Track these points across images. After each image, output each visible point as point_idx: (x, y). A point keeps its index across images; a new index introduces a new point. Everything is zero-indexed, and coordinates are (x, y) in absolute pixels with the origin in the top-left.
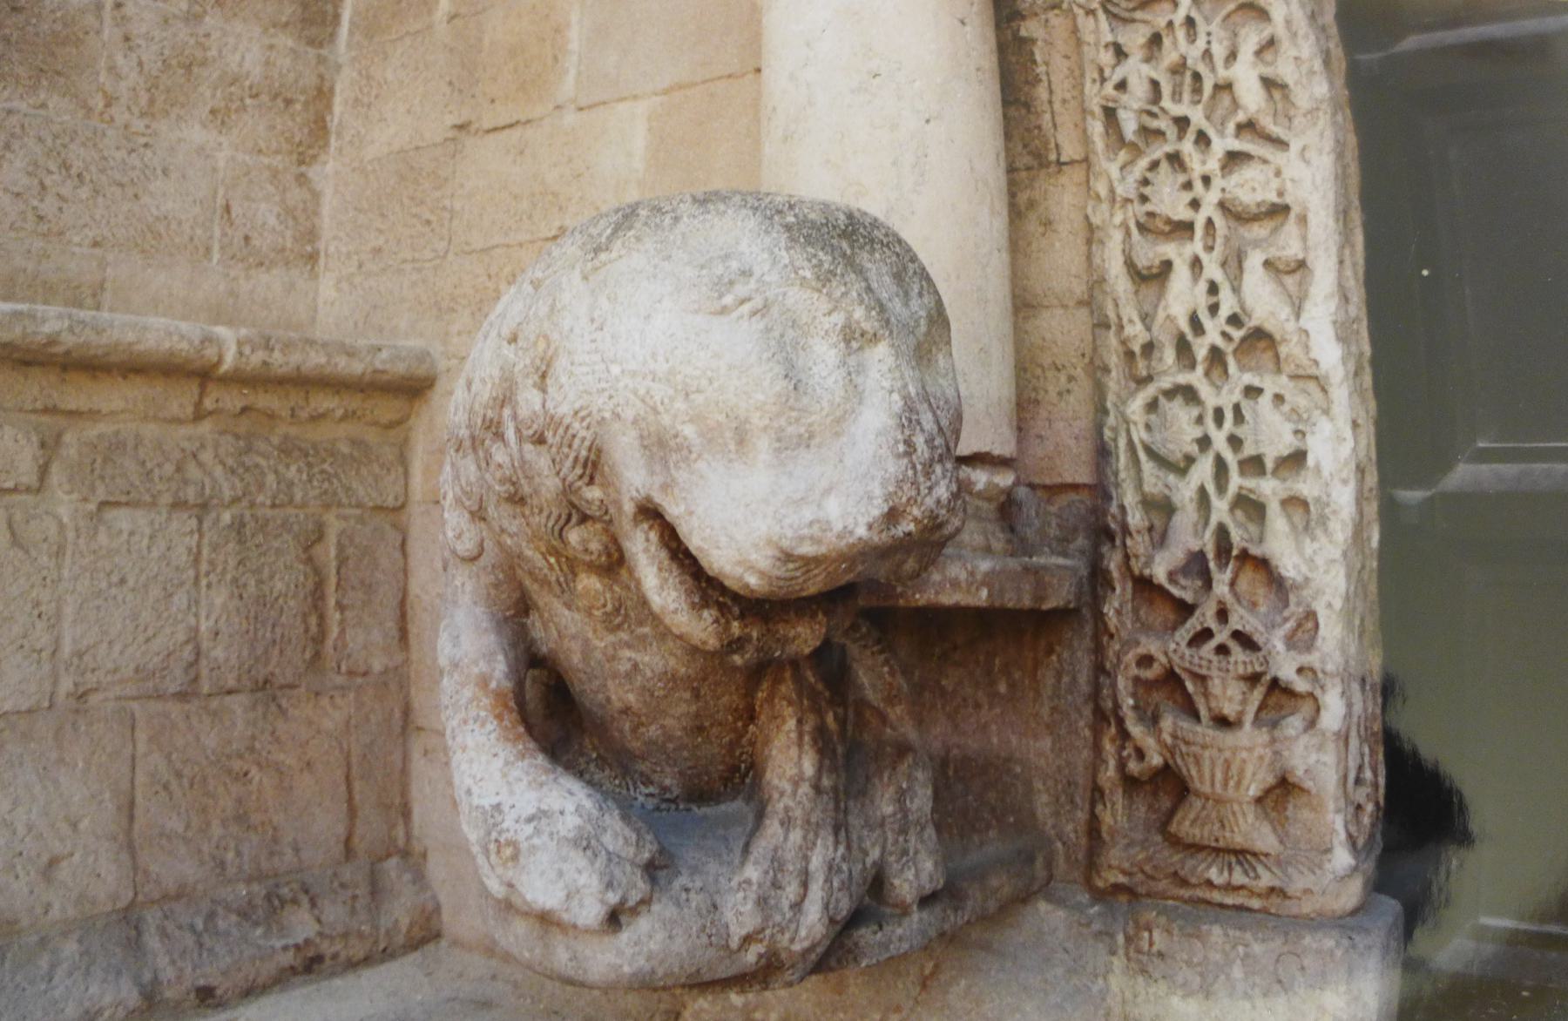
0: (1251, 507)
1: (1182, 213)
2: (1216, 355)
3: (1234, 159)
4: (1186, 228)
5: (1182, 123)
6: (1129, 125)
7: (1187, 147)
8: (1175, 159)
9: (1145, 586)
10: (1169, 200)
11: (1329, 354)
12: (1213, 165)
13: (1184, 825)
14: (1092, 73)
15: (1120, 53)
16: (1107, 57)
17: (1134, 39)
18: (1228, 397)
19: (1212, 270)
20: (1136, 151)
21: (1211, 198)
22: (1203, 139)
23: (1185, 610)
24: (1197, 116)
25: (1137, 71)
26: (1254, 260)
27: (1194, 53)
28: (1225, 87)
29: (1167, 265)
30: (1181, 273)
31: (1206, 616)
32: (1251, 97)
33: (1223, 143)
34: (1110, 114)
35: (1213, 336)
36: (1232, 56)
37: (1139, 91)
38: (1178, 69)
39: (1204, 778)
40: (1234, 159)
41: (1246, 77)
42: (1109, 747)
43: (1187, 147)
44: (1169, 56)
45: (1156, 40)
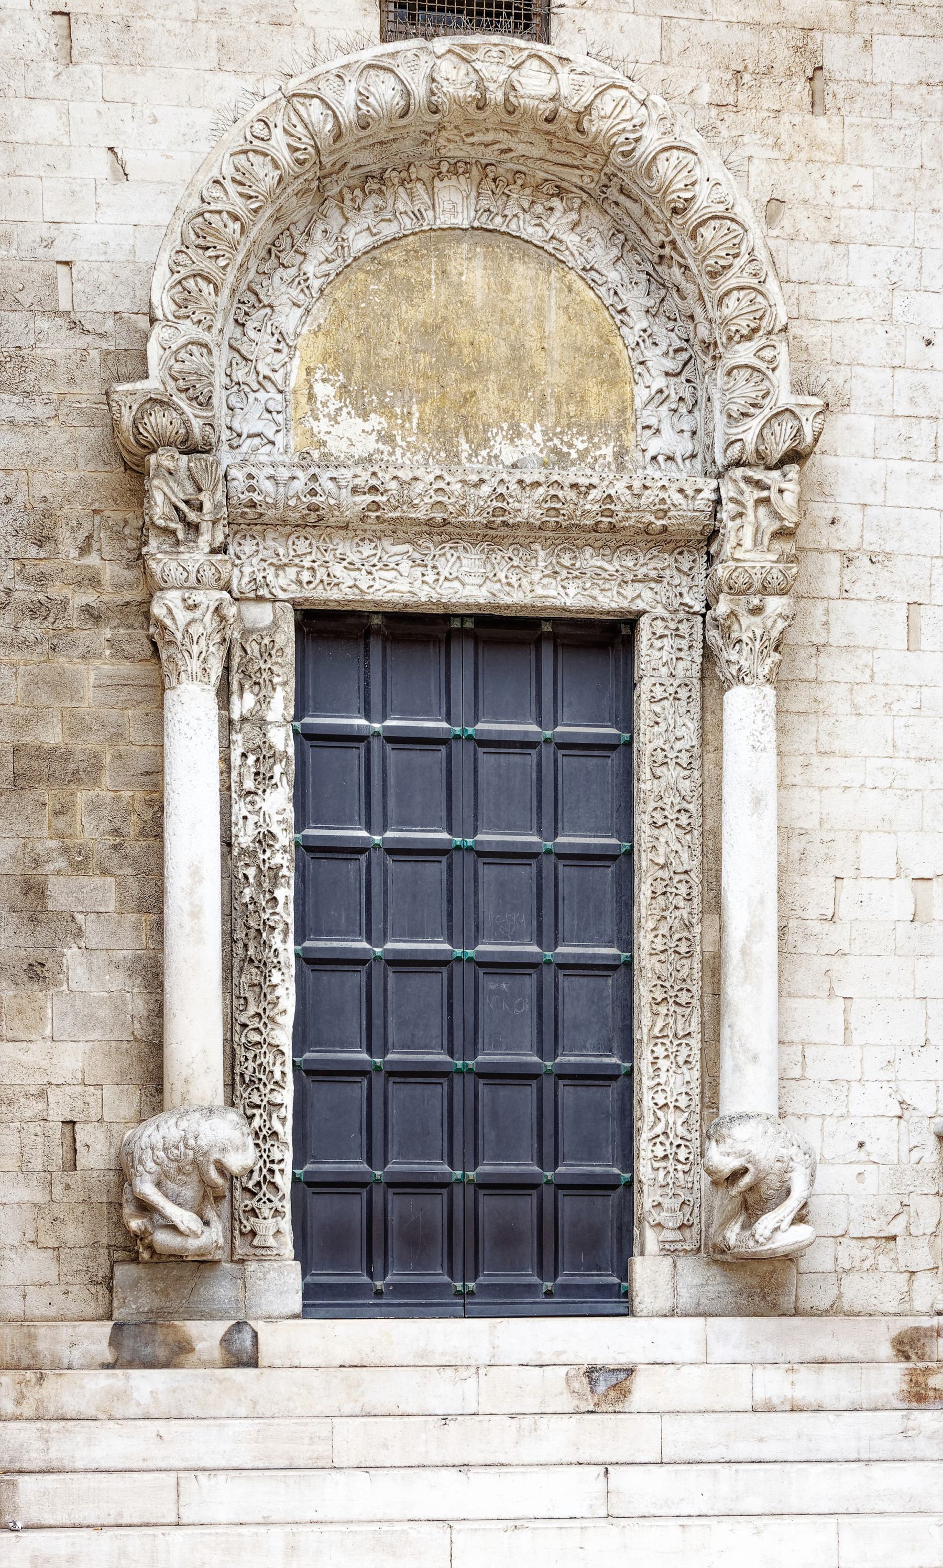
0: (271, 1171)
1: (259, 1103)
2: (265, 1137)
3: (272, 1090)
4: (259, 1107)
5: (260, 1080)
6: (247, 1080)
7: (261, 1086)
8: (258, 1089)
9: (246, 1189)
10: (256, 1099)
11: (289, 1139)
12: (267, 1091)
13: (255, 1242)
14: (237, 1062)
15: (247, 1059)
16: (243, 1059)
17: (250, 1055)
18: (267, 1147)
19: (265, 1117)
20: (248, 1086)
21: (266, 1100)
22: (265, 1085)
23: (254, 1194)
24: (264, 1078)
25: (250, 1065)
26: (274, 1116)
27: (265, 1061)
28: (272, 1072)
29: (254, 1115)
30: (257, 1118)
31: (261, 1195)
32: (278, 1076)
33: (270, 1086)
34: (242, 1075)
35: (264, 1132)
36: (274, 1064)
37: (251, 1069)
38: (261, 1065)
39: (260, 1230)
40: (272, 1090)
41: (277, 1071)
42: (237, 1227)
43: (261, 1086)
44: (258, 1062)
45: (255, 1056)
